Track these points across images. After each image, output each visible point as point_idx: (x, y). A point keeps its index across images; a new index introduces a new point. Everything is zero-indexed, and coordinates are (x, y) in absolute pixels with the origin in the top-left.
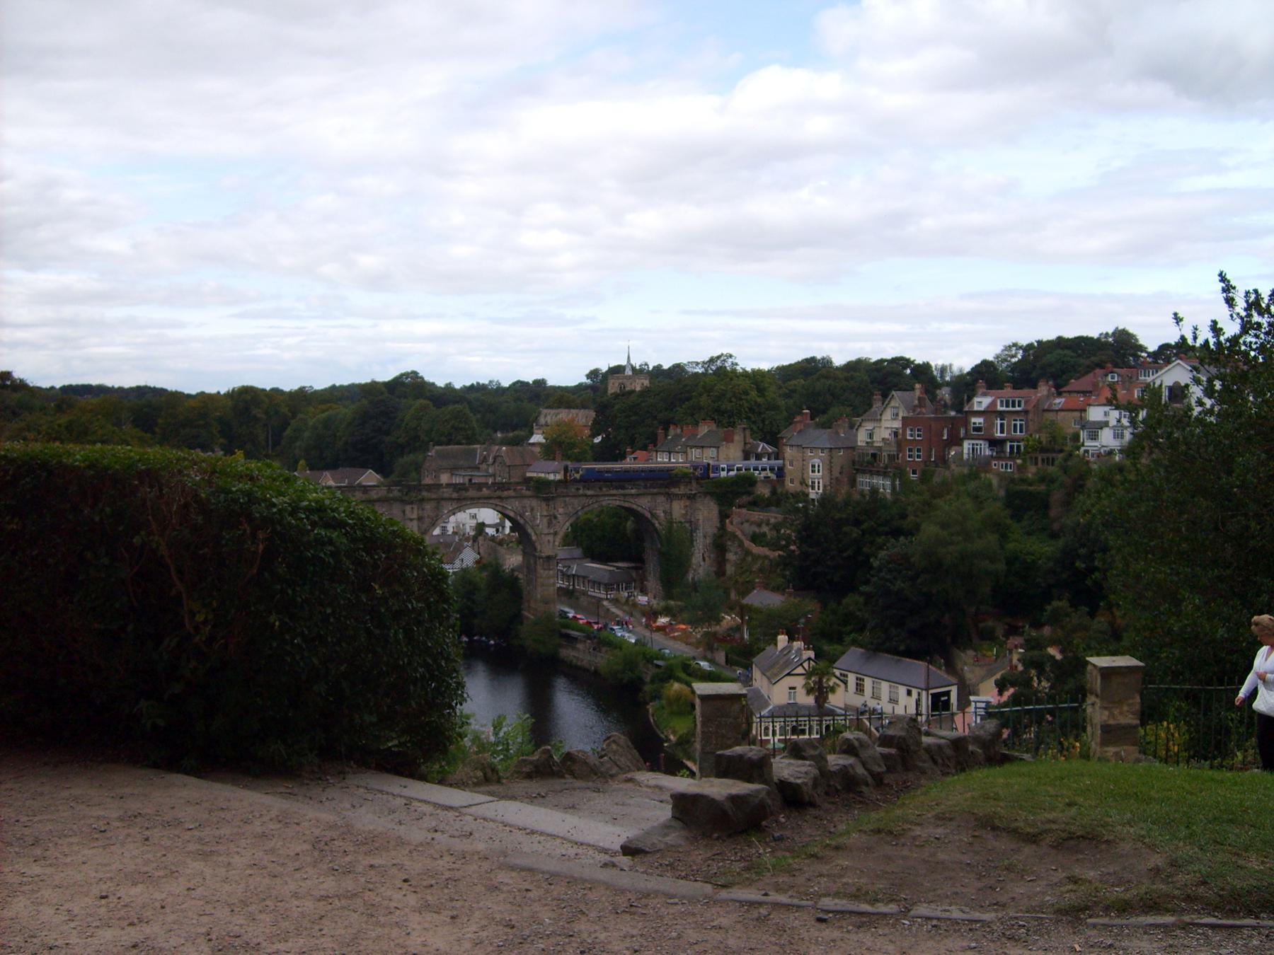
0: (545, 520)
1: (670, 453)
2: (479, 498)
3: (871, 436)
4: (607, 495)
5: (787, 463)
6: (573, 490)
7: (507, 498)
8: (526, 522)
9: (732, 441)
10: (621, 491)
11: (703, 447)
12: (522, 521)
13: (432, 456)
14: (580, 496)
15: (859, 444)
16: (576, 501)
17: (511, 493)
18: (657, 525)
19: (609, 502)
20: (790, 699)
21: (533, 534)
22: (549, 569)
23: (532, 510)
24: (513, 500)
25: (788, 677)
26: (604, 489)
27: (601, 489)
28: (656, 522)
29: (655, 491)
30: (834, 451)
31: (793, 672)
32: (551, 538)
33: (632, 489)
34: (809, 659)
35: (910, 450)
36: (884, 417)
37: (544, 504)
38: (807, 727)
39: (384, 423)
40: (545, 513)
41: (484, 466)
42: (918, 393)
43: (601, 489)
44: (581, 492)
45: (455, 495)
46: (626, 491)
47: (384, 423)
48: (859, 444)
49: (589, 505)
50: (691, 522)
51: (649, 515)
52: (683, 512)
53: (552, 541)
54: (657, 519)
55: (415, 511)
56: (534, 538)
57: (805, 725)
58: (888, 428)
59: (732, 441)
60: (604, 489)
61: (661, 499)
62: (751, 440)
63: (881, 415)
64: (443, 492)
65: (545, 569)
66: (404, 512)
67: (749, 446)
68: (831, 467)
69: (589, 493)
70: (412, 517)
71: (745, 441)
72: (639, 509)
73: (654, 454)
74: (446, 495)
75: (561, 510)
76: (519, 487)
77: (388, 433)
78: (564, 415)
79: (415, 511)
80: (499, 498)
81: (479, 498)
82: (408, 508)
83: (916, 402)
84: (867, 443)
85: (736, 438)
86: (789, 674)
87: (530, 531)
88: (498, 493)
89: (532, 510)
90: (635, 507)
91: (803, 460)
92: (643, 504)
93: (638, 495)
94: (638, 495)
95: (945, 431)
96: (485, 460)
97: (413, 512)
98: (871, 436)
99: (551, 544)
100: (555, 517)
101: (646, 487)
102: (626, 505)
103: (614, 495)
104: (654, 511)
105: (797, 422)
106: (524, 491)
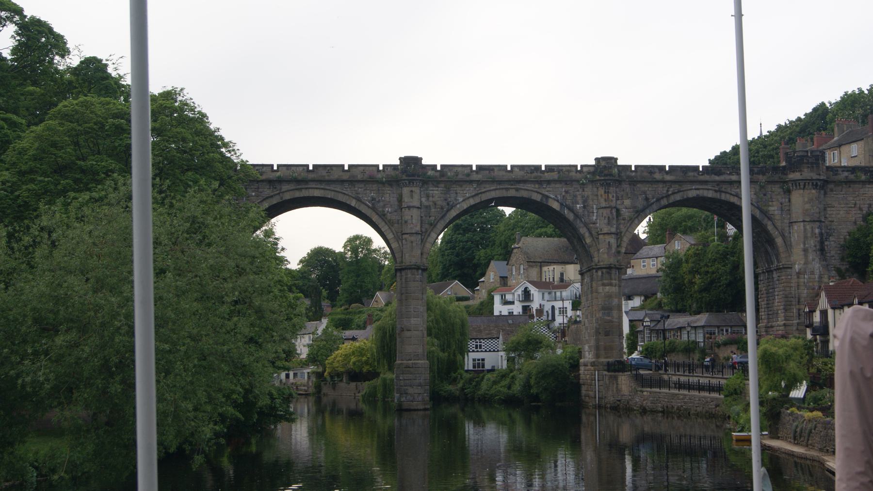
4: (692, 182)
7: (549, 182)
8: (577, 216)
10: (717, 178)
11: (840, 146)
12: (571, 216)
18: (770, 227)
19: (698, 192)
21: (587, 235)
22: (611, 285)
24: (558, 185)
28: (769, 223)
32: (613, 240)
33: (730, 174)
37: (601, 191)
40: (604, 204)
46: (722, 178)
49: (668, 196)
50: (820, 221)
52: (807, 206)
53: (614, 246)
54: (770, 219)
55: (416, 196)
56: (588, 240)
61: (777, 188)
65: (604, 285)
70: (411, 204)
75: (627, 202)
79: (416, 196)
82: (406, 191)
87: (583, 231)
97: (412, 197)
99: (613, 250)
102: (723, 197)
103: (705, 182)
106: (571, 174)
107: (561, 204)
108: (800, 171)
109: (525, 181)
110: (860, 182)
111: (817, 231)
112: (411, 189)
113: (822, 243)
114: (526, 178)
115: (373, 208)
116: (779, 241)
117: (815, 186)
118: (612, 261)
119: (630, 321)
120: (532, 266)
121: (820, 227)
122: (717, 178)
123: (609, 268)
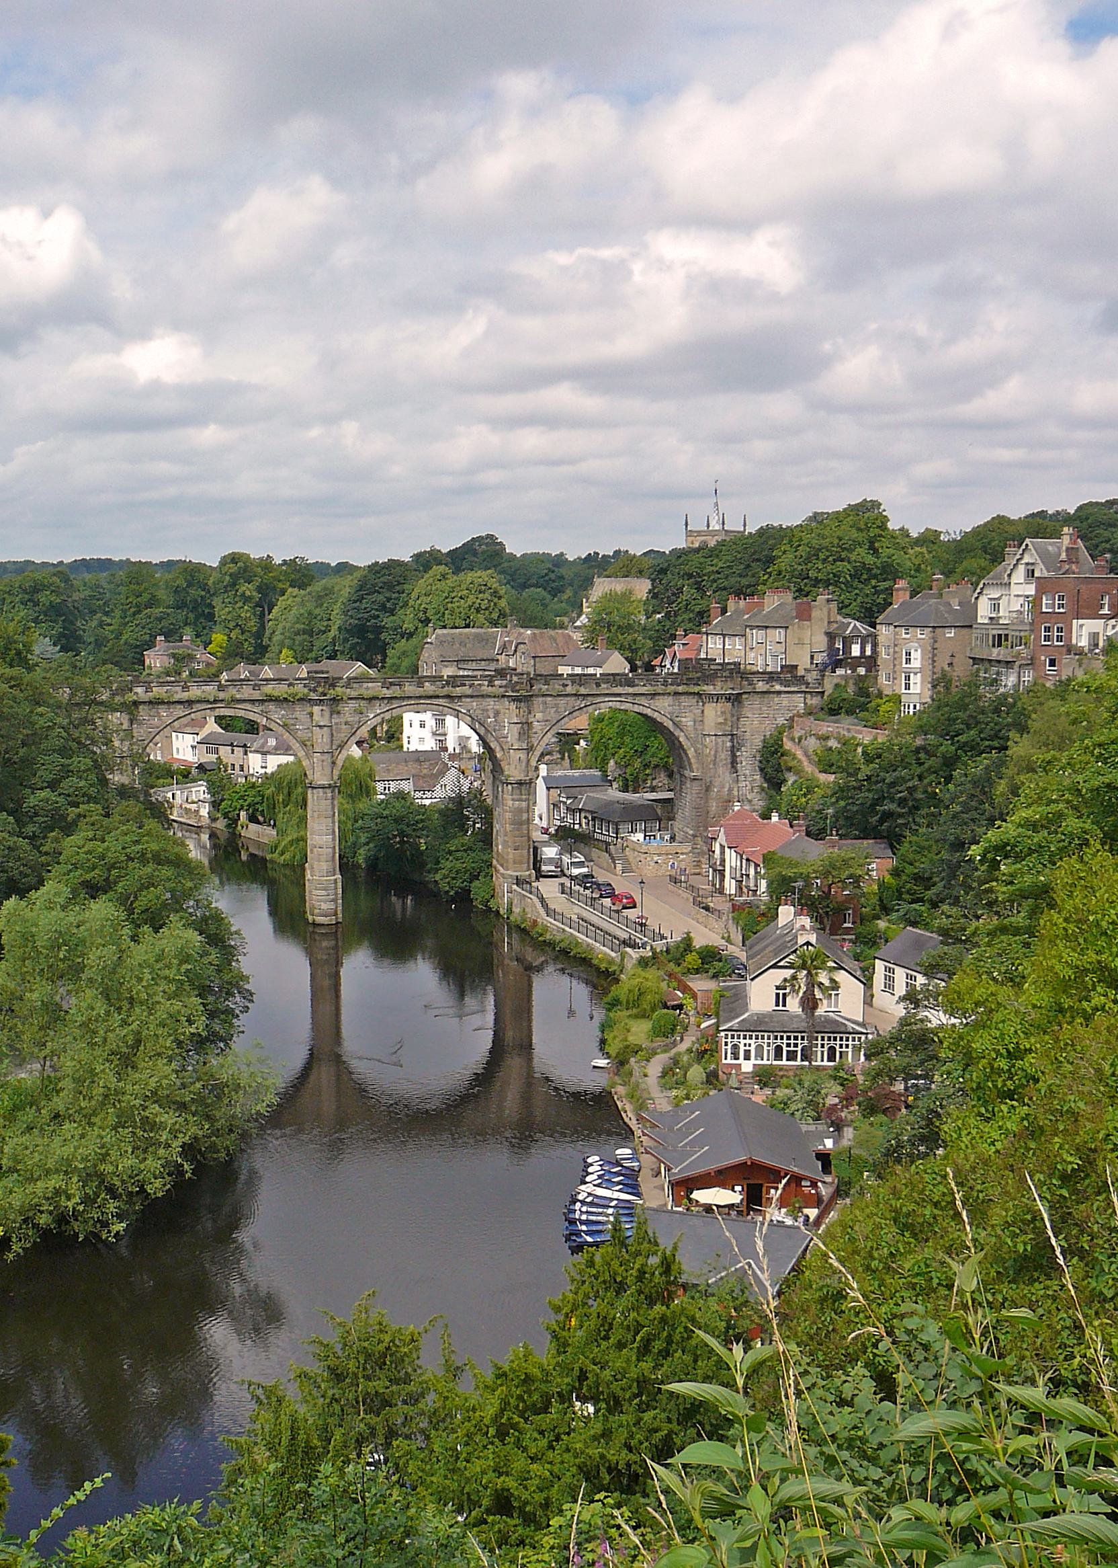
0: (515, 729)
1: (724, 636)
2: (420, 697)
3: (996, 607)
5: (882, 651)
6: (557, 686)
9: (809, 619)
10: (631, 690)
13: (431, 643)
14: (567, 695)
15: (979, 621)
16: (562, 702)
17: (467, 690)
20: (777, 1005)
23: (497, 713)
25: (771, 970)
26: (603, 686)
27: (598, 685)
28: (682, 734)
29: (680, 689)
30: (938, 630)
31: (780, 964)
32: (523, 755)
33: (644, 685)
34: (808, 944)
35: (1047, 629)
36: (1014, 580)
38: (799, 1048)
39: (389, 600)
41: (502, 658)
42: (1066, 541)
43: (598, 685)
44: (569, 690)
45: (387, 693)
47: (389, 600)
48: (979, 621)
51: (669, 724)
52: (721, 720)
57: (796, 1045)
58: (1018, 596)
59: (809, 619)
60: (603, 686)
62: (839, 618)
63: (1009, 575)
64: (367, 688)
65: (513, 800)
66: (311, 714)
67: (835, 625)
68: (934, 655)
69: (583, 691)
71: (829, 618)
72: (656, 715)
73: (705, 637)
74: (370, 694)
75: (539, 716)
76: (476, 683)
77: (392, 612)
78: (618, 586)
79: (327, 714)
80: (448, 697)
81: (420, 697)
82: (316, 709)
83: (1063, 556)
84: (991, 618)
85: (815, 614)
86: (774, 966)
88: (447, 690)
89: (497, 713)
90: (648, 712)
91: (896, 645)
92: (662, 709)
93: (654, 695)
94: (653, 695)
95: (1106, 600)
96: (504, 647)
98: (996, 607)
100: (529, 724)
101: (665, 684)
103: (619, 695)
104: (678, 719)
105: (898, 590)
106: (483, 688)
107: (473, 719)
108: (714, 685)
109: (437, 697)
110: (774, 692)
111: (729, 744)
112: (321, 708)
113: (734, 756)
114: (437, 693)
115: (285, 726)
116: (691, 752)
117: (728, 698)
118: (522, 777)
119: (548, 789)
120: (447, 667)
121: (732, 741)
122: (631, 690)
123: (520, 783)
